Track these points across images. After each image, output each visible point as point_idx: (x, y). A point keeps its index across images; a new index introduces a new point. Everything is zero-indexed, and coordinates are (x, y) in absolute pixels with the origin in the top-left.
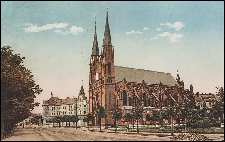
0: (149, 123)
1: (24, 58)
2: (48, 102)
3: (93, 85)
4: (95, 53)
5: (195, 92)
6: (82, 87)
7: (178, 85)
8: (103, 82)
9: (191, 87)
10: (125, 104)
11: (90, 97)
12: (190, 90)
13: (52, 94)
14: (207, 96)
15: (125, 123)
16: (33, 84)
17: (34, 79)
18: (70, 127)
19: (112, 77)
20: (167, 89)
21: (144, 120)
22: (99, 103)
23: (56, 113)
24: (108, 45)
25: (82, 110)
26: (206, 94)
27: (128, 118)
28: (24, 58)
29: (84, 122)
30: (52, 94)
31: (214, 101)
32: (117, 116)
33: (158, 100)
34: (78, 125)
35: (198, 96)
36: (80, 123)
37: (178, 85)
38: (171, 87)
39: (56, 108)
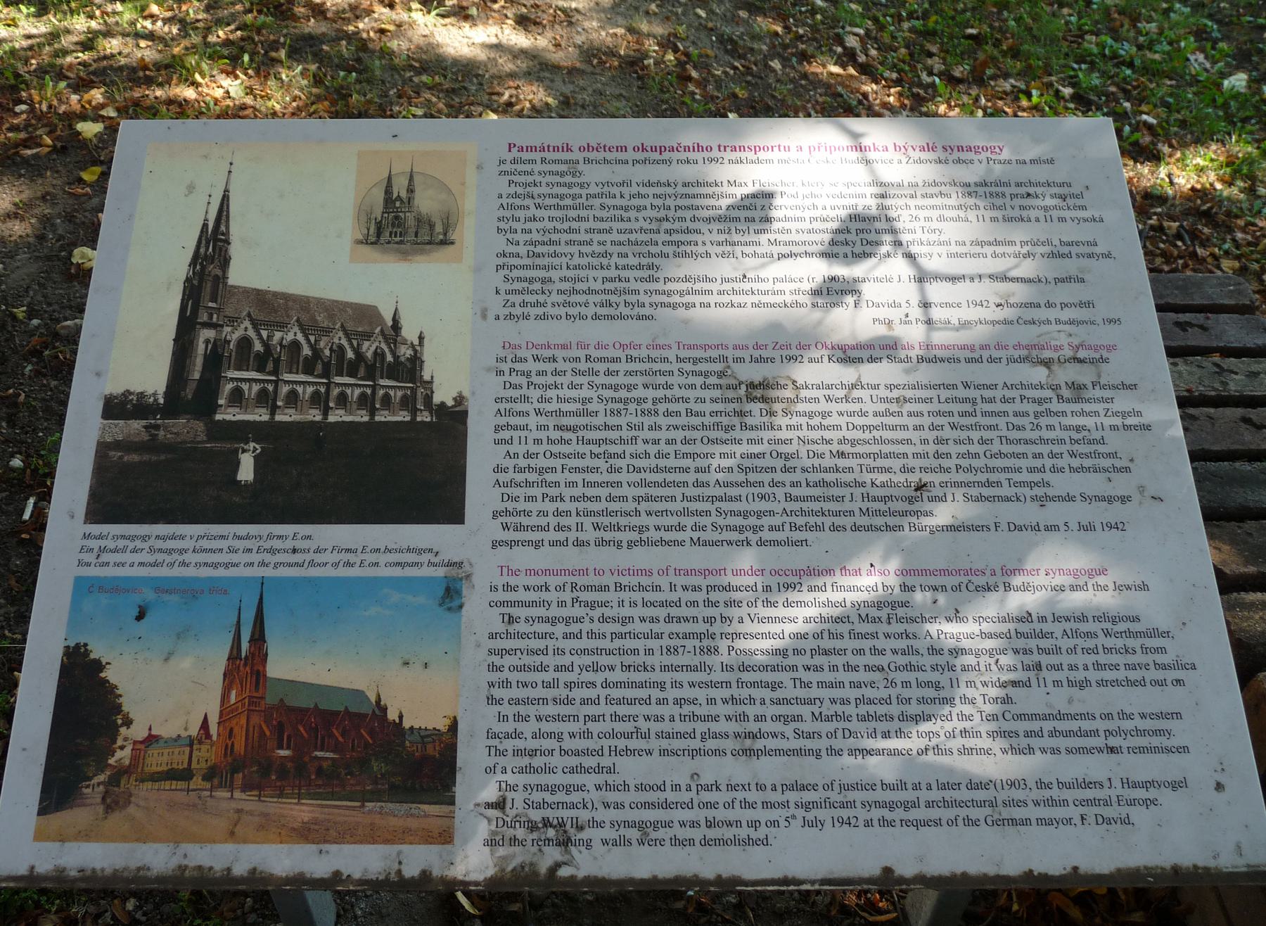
0: (320, 782)
1: (109, 663)
2: (141, 742)
3: (226, 714)
4: (234, 656)
5: (407, 724)
6: (206, 715)
7: (377, 712)
8: (243, 705)
9: (401, 717)
10: (281, 747)
11: (219, 735)
12: (397, 721)
13: (150, 729)
14: (429, 733)
15: (278, 784)
16: (118, 709)
17: (121, 700)
18: (176, 790)
19: (187, 750)
20: (356, 719)
21: (313, 777)
22: (233, 745)
23: (154, 763)
24: (259, 638)
25: (205, 756)
26: (426, 729)
27: (283, 774)
28: (109, 663)
29: (203, 780)
30: (150, 729)
31: (441, 742)
32: (265, 770)
33: (341, 739)
34: (191, 787)
35: (412, 733)
36: (197, 782)
37: (377, 712)
38: (365, 716)
39: (156, 755)
